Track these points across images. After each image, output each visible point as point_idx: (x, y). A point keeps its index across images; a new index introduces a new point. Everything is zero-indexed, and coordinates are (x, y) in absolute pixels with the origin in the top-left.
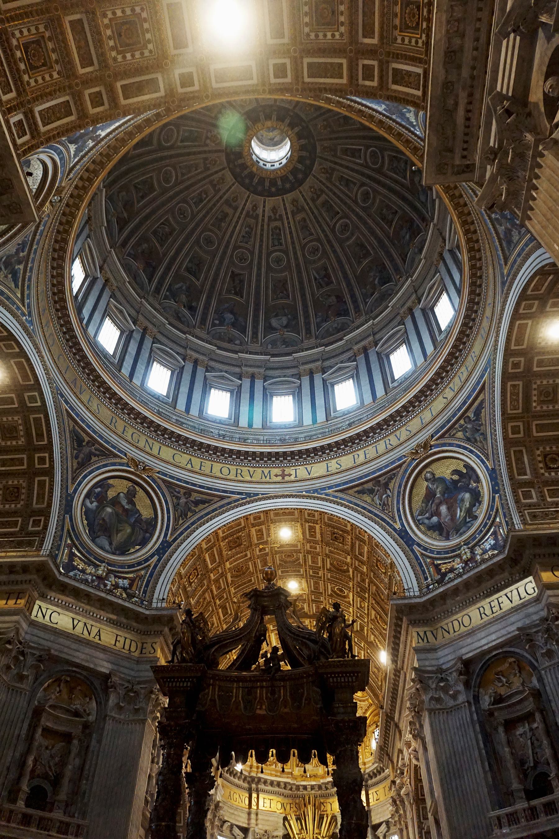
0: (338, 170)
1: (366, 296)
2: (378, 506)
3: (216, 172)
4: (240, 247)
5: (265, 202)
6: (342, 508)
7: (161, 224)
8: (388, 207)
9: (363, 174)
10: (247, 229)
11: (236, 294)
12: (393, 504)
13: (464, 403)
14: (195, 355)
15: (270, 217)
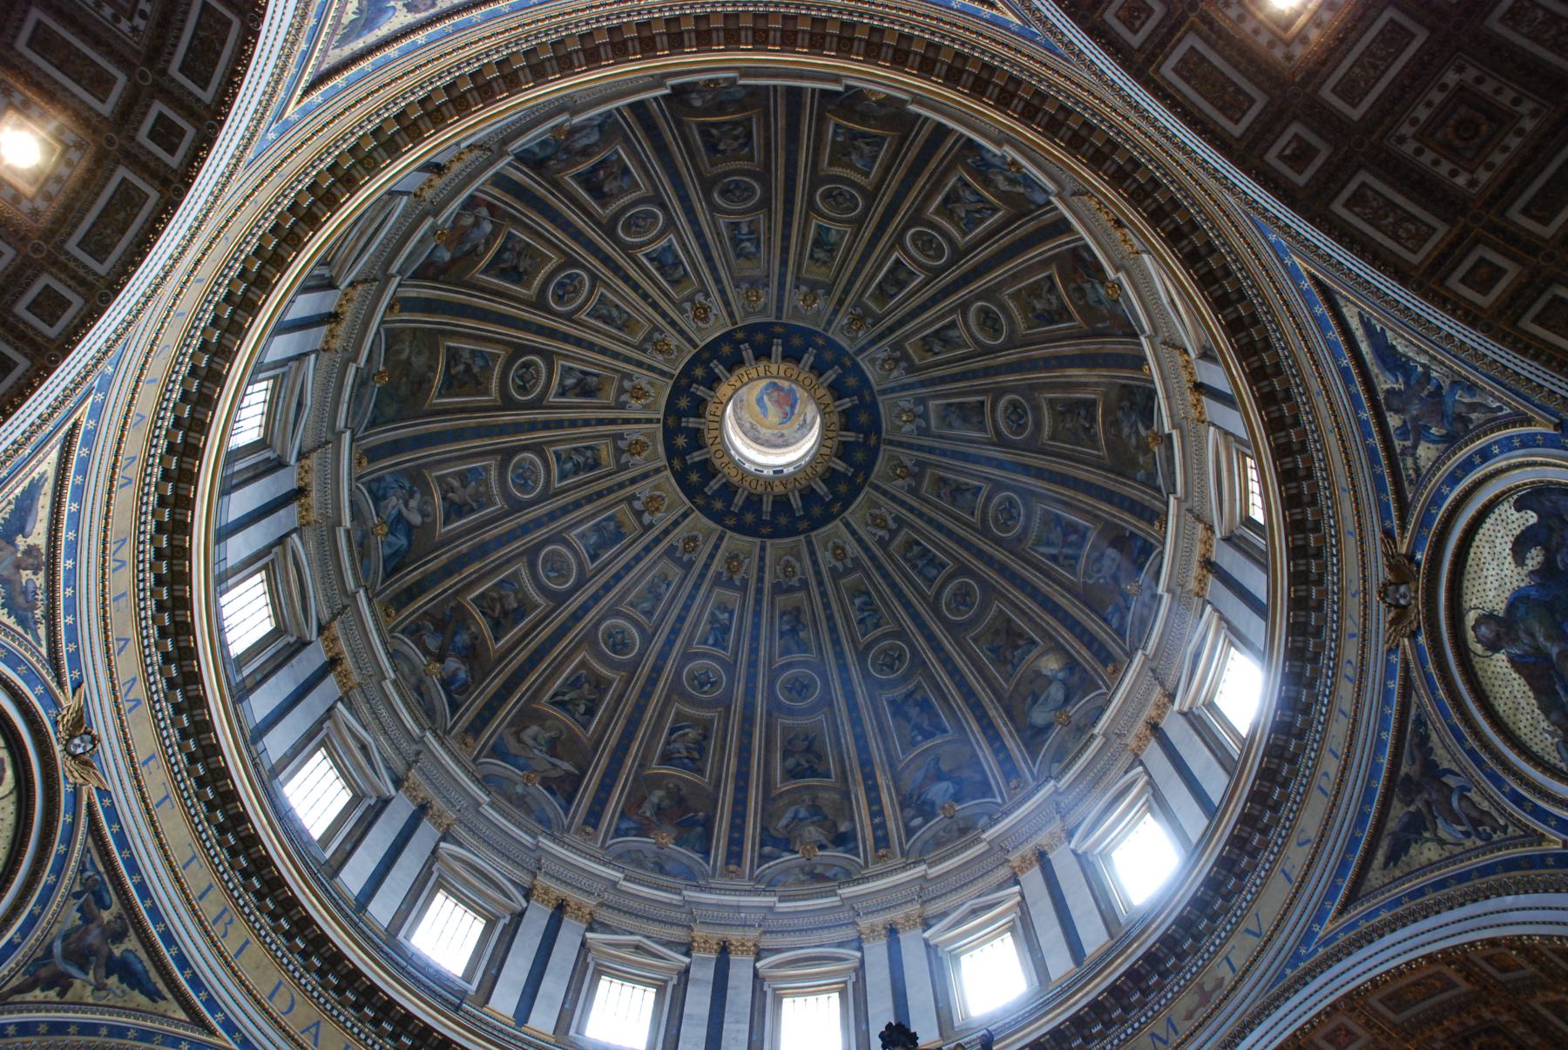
0: (907, 337)
1: (1150, 482)
2: (1468, 843)
3: (712, 556)
4: (869, 646)
5: (847, 525)
6: (1389, 939)
7: (673, 731)
8: (1034, 290)
9: (946, 293)
10: (857, 601)
11: (928, 736)
12: (1489, 798)
13: (1344, 372)
14: (880, 919)
15: (883, 544)
